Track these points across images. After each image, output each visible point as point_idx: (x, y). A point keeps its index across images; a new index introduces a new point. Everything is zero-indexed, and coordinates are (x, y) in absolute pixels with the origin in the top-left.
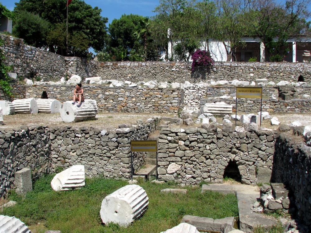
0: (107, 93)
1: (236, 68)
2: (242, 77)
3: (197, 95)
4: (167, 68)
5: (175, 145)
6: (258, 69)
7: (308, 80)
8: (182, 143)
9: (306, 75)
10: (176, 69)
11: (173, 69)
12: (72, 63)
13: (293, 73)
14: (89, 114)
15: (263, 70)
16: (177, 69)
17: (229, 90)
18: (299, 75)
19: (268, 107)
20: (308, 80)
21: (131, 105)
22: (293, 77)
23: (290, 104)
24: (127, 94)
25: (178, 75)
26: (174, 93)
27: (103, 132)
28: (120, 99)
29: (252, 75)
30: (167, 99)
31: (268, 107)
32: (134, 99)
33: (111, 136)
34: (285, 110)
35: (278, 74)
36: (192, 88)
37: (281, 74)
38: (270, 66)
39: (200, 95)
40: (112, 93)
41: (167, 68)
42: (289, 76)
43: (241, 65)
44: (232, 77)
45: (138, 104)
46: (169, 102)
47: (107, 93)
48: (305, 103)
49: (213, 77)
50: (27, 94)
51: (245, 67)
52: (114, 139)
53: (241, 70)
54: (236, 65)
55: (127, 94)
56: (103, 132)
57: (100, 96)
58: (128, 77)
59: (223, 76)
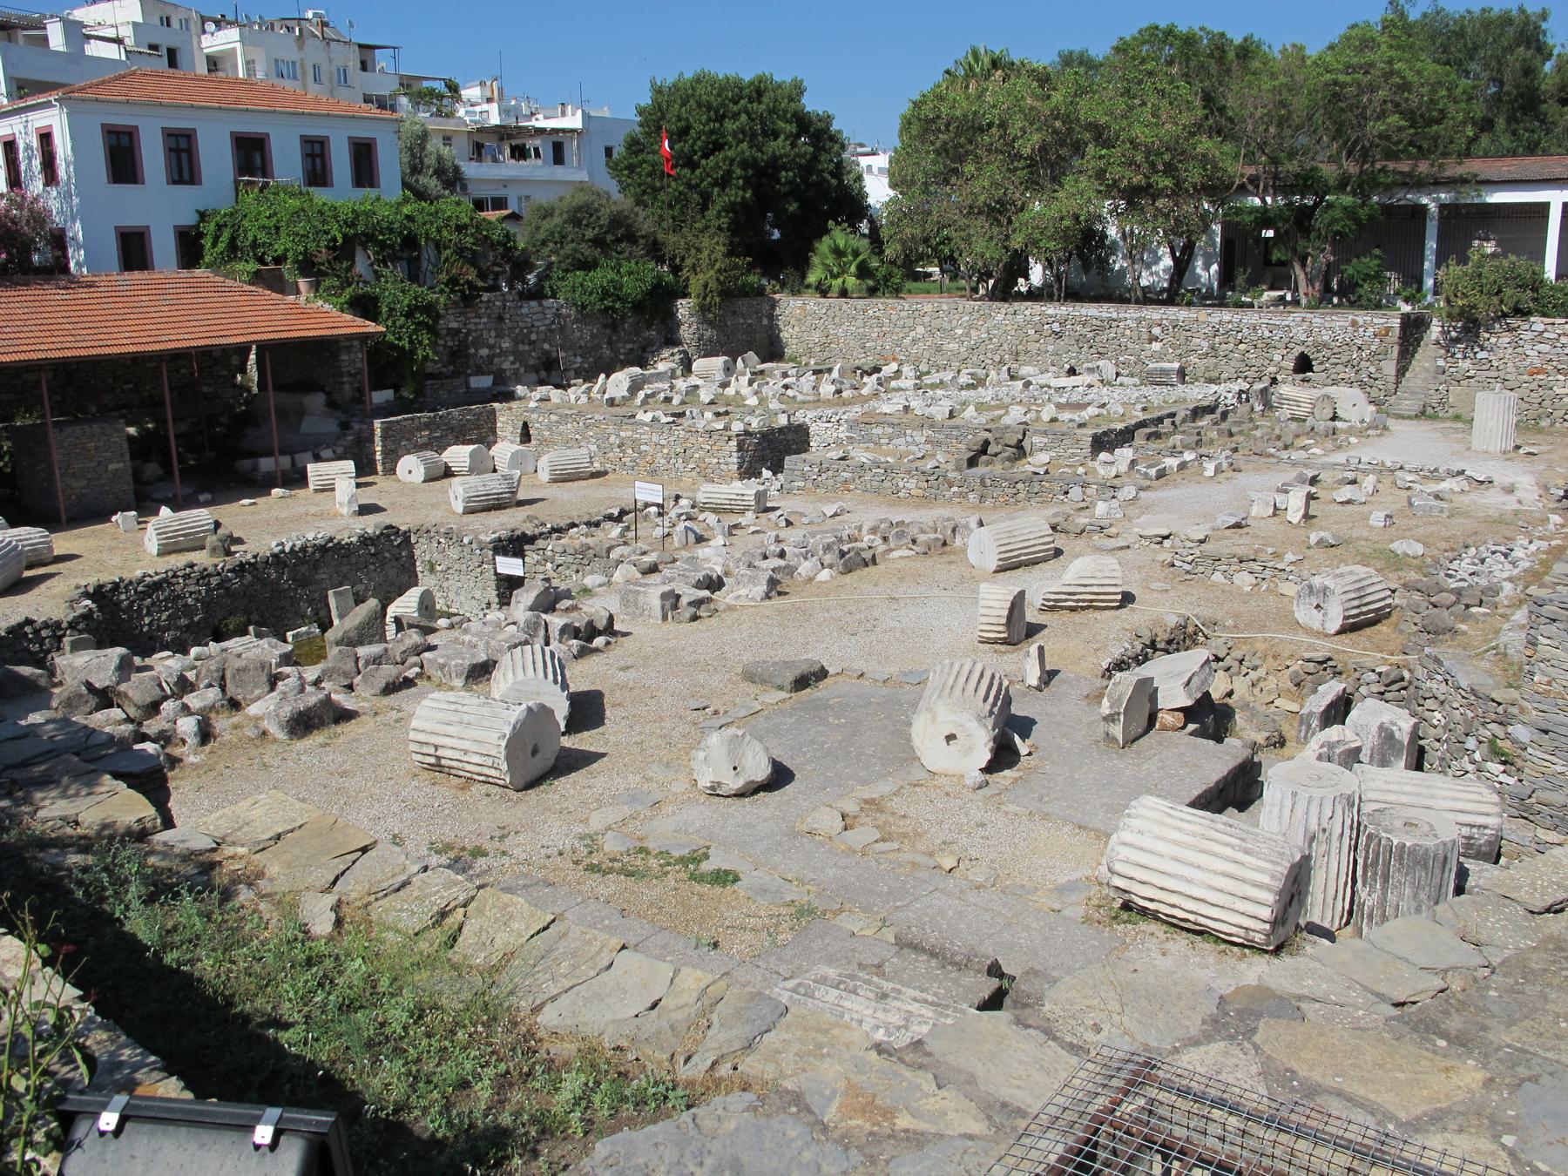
0: (623, 434)
1: (1114, 324)
2: (1129, 351)
3: (835, 435)
5: (541, 569)
6: (1174, 327)
7: (1322, 367)
8: (549, 565)
9: (1319, 351)
14: (498, 499)
15: (1189, 334)
17: (890, 430)
20: (1322, 367)
22: (1277, 358)
23: (956, 483)
26: (731, 443)
30: (720, 453)
32: (665, 451)
33: (474, 546)
34: (948, 495)
35: (1231, 346)
37: (1242, 347)
40: (629, 433)
43: (1127, 316)
44: (1100, 350)
47: (623, 434)
48: (988, 482)
49: (1051, 348)
50: (499, 425)
51: (1139, 321)
52: (478, 552)
53: (1128, 332)
54: (1114, 315)
57: (612, 439)
59: (1076, 348)
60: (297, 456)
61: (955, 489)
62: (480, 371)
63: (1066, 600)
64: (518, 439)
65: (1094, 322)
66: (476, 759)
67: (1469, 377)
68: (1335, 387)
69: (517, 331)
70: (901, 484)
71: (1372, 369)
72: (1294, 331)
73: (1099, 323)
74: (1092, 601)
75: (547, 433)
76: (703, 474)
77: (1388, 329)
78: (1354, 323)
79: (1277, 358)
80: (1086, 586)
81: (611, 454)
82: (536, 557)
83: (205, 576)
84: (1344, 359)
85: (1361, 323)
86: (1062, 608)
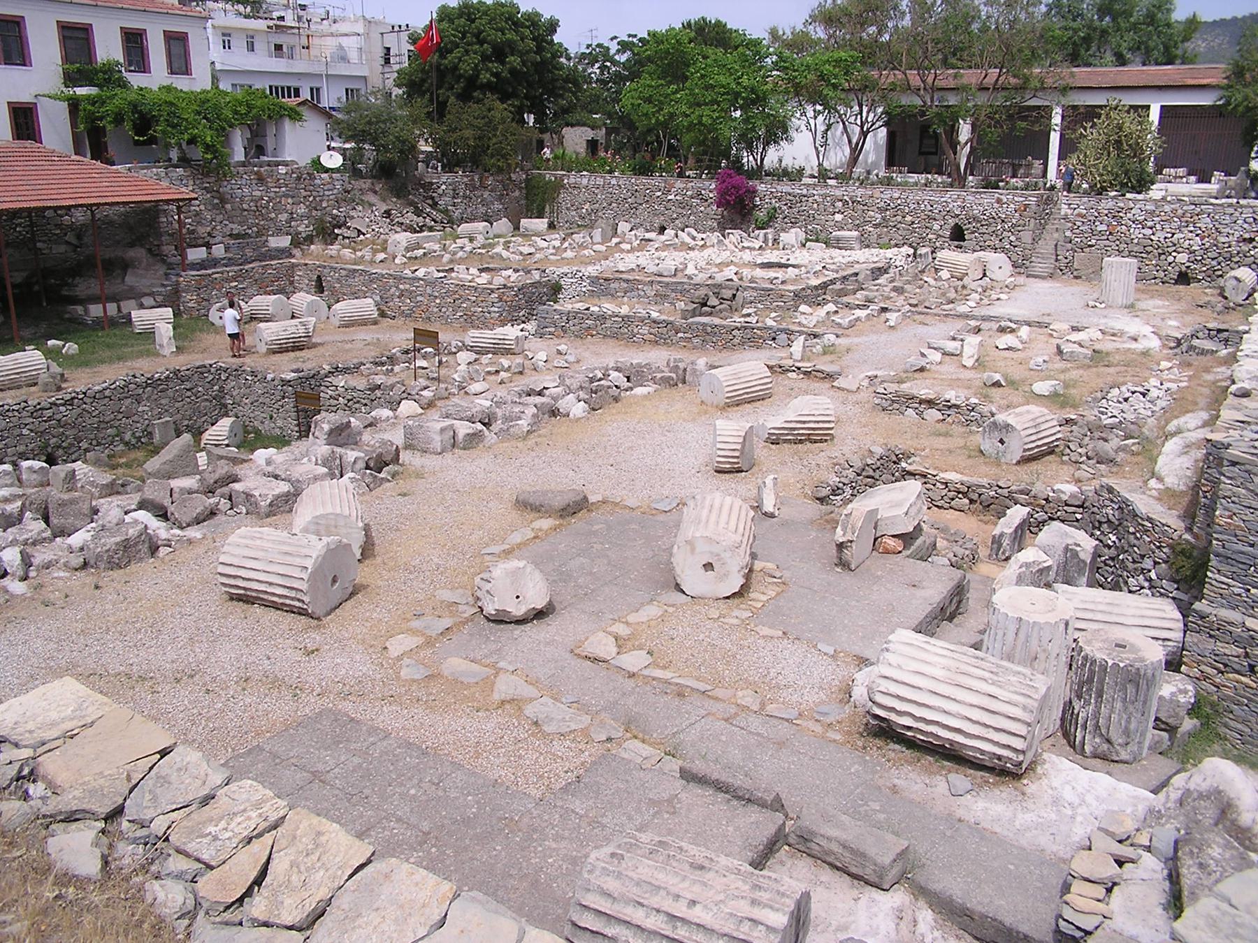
0: (401, 287)
1: (804, 199)
4: (659, 194)
10: (678, 198)
11: (669, 197)
12: (444, 187)
13: (937, 217)
16: (678, 198)
17: (626, 285)
18: (952, 222)
19: (646, 332)
21: (436, 310)
22: (936, 227)
24: (429, 290)
25: (680, 210)
27: (270, 377)
28: (419, 298)
29: (838, 217)
31: (646, 332)
32: (438, 301)
33: (276, 382)
35: (899, 218)
36: (569, 275)
38: (882, 196)
39: (584, 289)
41: (659, 194)
42: (927, 225)
43: (815, 192)
45: (443, 310)
46: (485, 310)
54: (805, 192)
55: (429, 290)
56: (270, 377)
58: (584, 211)
60: (122, 304)
61: (680, 335)
62: (279, 232)
63: (787, 434)
64: (313, 290)
65: (789, 197)
66: (279, 591)
67: (1090, 246)
68: (982, 252)
69: (311, 199)
70: (636, 330)
71: (1013, 238)
72: (951, 206)
73: (791, 198)
74: (809, 434)
75: (337, 285)
76: (469, 320)
77: (1026, 206)
78: (999, 201)
79: (936, 227)
80: (804, 422)
81: (391, 304)
82: (330, 392)
83: (37, 411)
84: (991, 229)
85: (1005, 200)
86: (786, 441)
